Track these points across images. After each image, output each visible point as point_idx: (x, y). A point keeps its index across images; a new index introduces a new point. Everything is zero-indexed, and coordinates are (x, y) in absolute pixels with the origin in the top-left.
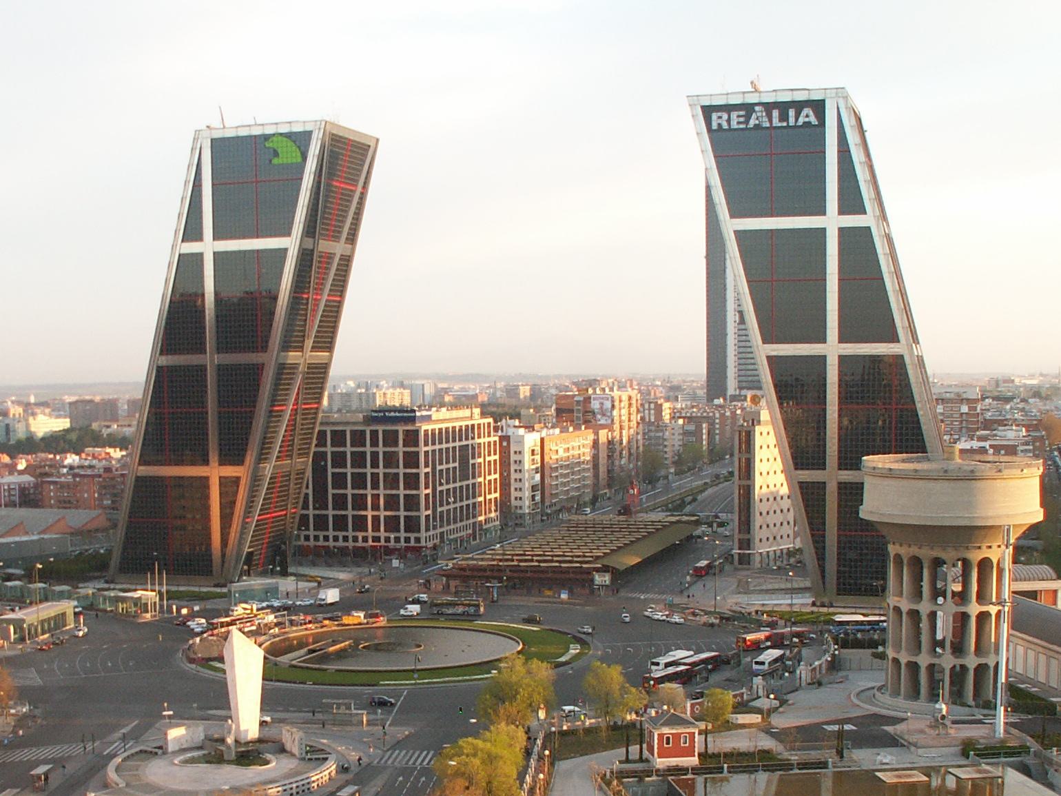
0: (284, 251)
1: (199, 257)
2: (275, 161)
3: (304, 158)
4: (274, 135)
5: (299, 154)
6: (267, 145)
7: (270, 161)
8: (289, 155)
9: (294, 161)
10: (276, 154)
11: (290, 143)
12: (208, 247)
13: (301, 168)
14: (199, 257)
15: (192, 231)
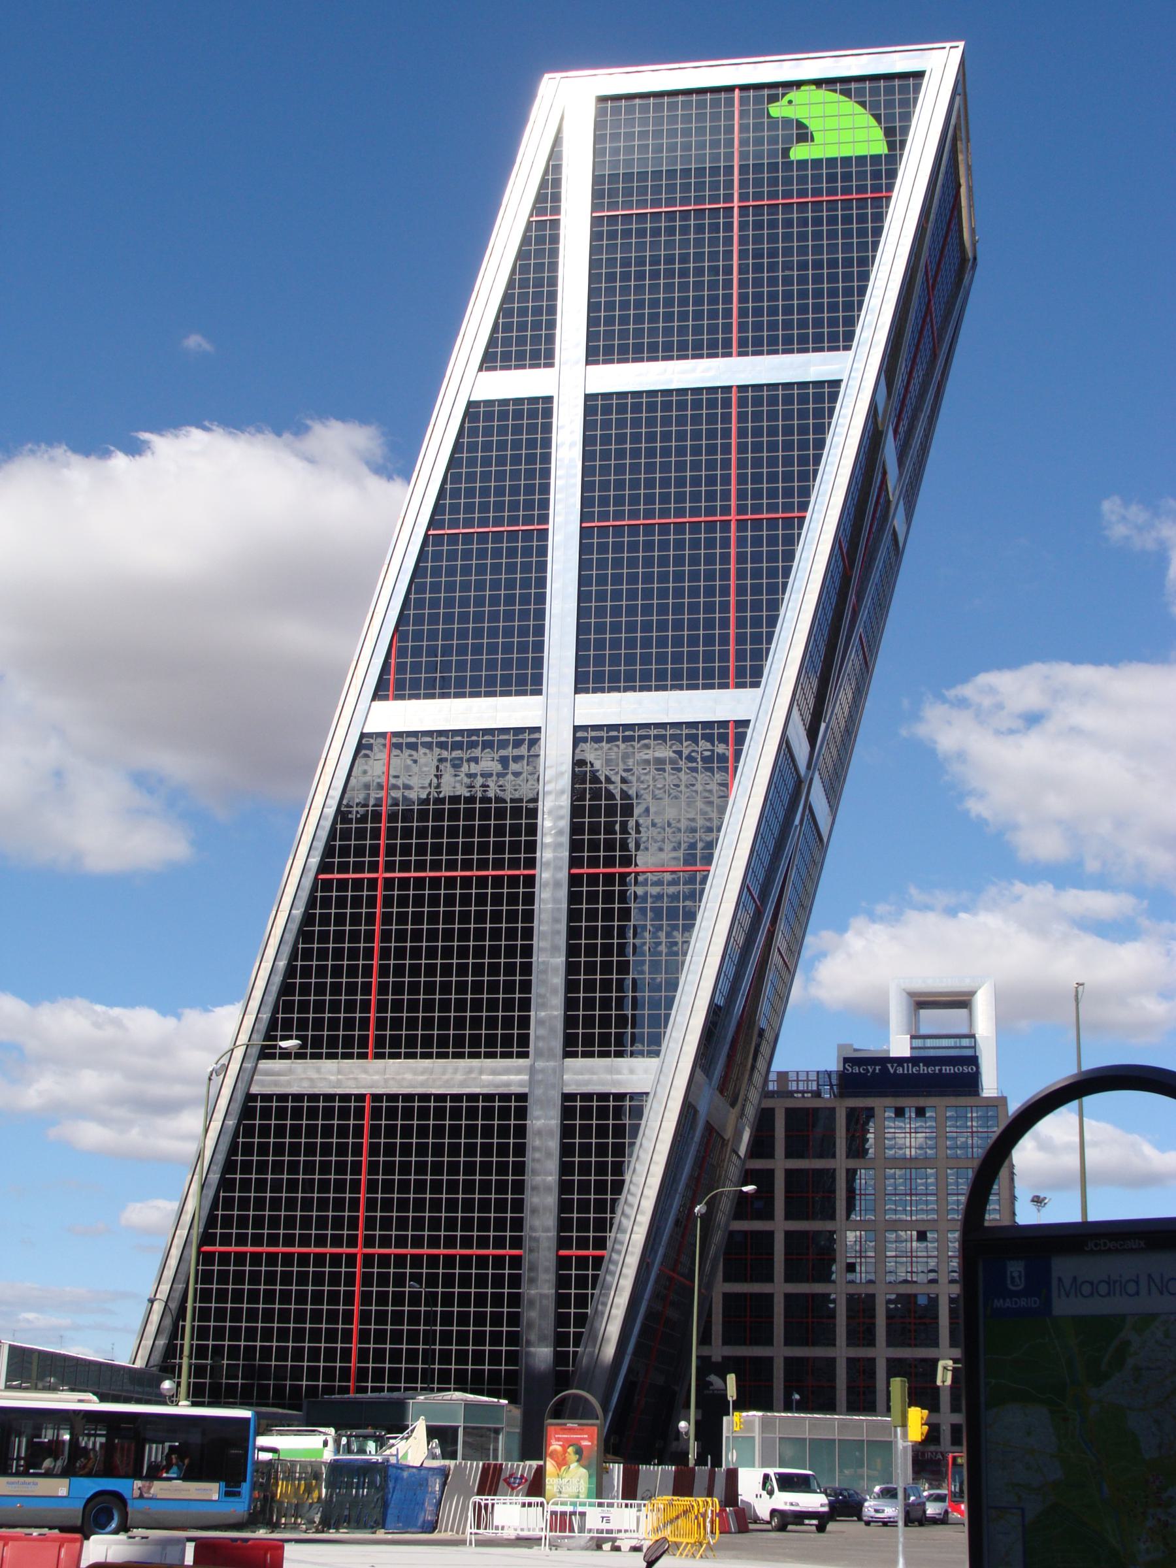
0: (826, 393)
1: (539, 410)
2: (799, 152)
3: (896, 136)
4: (798, 84)
5: (878, 133)
6: (777, 110)
7: (786, 152)
8: (846, 136)
9: (861, 150)
10: (804, 135)
11: (849, 106)
12: (570, 380)
13: (880, 173)
14: (539, 410)
15: (523, 335)
